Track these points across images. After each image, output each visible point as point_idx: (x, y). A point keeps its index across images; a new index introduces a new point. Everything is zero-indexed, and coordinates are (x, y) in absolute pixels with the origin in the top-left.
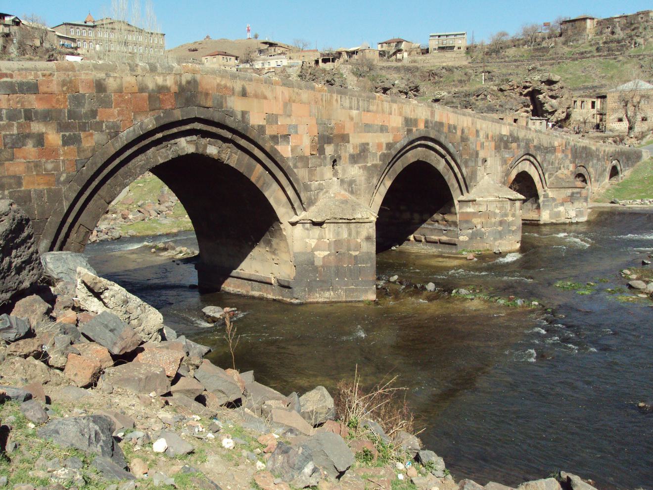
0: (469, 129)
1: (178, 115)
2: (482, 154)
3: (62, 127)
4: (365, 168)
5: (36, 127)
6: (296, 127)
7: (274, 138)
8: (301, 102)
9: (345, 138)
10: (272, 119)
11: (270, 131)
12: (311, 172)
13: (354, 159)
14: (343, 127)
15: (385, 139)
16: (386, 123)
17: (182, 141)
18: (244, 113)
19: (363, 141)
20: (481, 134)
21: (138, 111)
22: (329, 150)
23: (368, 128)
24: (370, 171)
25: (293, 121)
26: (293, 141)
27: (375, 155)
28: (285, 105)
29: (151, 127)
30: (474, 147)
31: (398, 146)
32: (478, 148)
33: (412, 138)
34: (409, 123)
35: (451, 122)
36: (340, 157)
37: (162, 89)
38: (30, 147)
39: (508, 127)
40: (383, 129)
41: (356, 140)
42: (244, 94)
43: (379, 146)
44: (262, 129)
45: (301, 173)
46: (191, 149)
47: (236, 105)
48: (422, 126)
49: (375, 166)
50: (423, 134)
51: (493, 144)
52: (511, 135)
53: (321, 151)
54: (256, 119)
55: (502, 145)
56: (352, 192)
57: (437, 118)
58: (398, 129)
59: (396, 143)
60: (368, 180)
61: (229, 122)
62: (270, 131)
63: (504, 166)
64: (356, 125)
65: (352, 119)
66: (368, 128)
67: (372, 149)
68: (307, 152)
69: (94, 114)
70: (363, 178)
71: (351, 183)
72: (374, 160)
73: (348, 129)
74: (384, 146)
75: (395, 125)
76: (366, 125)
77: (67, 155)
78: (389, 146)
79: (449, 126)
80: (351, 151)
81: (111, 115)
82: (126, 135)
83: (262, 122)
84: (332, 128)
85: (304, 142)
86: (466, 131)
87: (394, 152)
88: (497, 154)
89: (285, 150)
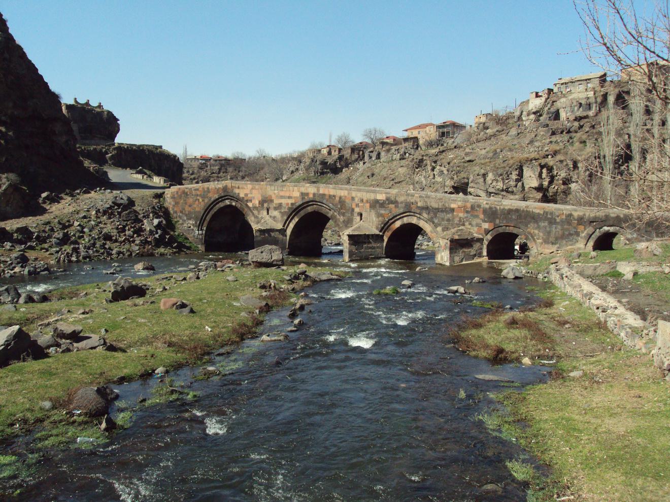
0: (346, 197)
1: (223, 195)
2: (357, 210)
3: (202, 198)
4: (281, 212)
5: (198, 198)
6: (254, 197)
7: (247, 201)
11: (245, 199)
13: (276, 209)
15: (290, 201)
17: (227, 201)
18: (239, 193)
19: (280, 202)
20: (356, 200)
21: (215, 194)
22: (266, 205)
23: (282, 197)
24: (283, 214)
27: (285, 208)
29: (217, 197)
31: (297, 204)
33: (304, 201)
34: (303, 195)
35: (332, 193)
37: (219, 188)
38: (197, 202)
39: (384, 195)
40: (289, 197)
41: (276, 201)
42: (239, 188)
43: (287, 204)
44: (243, 198)
45: (255, 212)
46: (229, 203)
47: (237, 191)
48: (311, 196)
49: (285, 212)
50: (312, 199)
51: (368, 205)
52: (388, 199)
53: (263, 205)
54: (242, 195)
55: (378, 205)
56: (275, 221)
57: (321, 192)
58: (297, 197)
59: (295, 203)
60: (282, 217)
61: (235, 196)
62: (245, 199)
63: (380, 218)
64: (277, 196)
66: (282, 197)
67: (284, 205)
68: (257, 206)
71: (274, 217)
72: (285, 209)
73: (273, 197)
75: (296, 196)
76: (281, 196)
77: (202, 203)
78: (292, 204)
79: (330, 196)
82: (212, 199)
85: (256, 202)
86: (343, 198)
87: (295, 207)
89: (250, 205)
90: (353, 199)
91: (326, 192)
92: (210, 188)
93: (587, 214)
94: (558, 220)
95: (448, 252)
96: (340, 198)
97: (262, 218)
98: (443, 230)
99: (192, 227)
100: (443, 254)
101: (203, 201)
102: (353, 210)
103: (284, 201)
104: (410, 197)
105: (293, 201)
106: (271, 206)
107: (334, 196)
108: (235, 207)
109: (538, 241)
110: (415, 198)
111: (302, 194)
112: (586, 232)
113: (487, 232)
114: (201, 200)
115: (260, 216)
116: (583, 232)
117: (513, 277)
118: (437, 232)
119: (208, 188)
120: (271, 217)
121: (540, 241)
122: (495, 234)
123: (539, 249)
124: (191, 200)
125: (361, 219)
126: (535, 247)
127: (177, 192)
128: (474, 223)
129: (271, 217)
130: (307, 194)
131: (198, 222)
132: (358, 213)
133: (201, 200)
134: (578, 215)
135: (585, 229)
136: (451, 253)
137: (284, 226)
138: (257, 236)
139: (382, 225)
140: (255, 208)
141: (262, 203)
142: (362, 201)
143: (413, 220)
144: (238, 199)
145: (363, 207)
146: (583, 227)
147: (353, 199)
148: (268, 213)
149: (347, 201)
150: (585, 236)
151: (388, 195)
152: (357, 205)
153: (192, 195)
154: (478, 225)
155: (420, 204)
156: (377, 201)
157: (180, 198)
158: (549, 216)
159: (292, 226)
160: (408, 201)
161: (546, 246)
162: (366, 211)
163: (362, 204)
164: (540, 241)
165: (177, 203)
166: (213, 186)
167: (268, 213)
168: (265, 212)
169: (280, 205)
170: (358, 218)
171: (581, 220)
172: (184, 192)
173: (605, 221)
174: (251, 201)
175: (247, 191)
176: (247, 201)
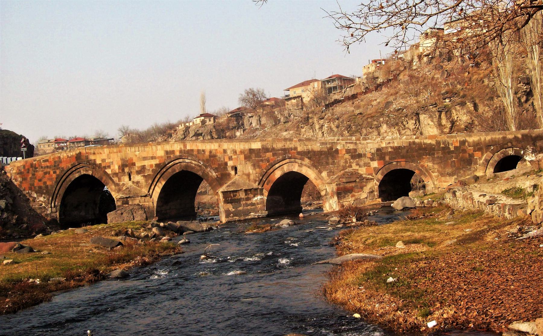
0: (216, 150)
2: (230, 163)
4: (144, 176)
7: (105, 167)
8: (114, 153)
9: (134, 164)
10: (104, 160)
11: (103, 165)
12: (120, 180)
13: (138, 173)
14: (132, 160)
15: (154, 162)
16: (155, 155)
20: (229, 152)
22: (126, 170)
23: (145, 159)
25: (111, 160)
26: (112, 168)
27: (149, 170)
28: (108, 155)
30: (222, 160)
32: (226, 160)
36: (131, 172)
40: (153, 158)
41: (138, 164)
42: (94, 154)
44: (100, 164)
45: (116, 179)
47: (92, 157)
51: (242, 157)
53: (123, 170)
54: (98, 162)
56: (138, 186)
57: (188, 147)
58: (162, 157)
60: (146, 181)
65: (136, 156)
66: (145, 159)
67: (147, 168)
69: (59, 165)
70: (143, 181)
71: (138, 183)
74: (154, 166)
75: (159, 155)
77: (54, 176)
78: (157, 165)
79: (198, 151)
80: (137, 169)
81: (63, 165)
83: (100, 162)
84: (127, 161)
85: (116, 168)
88: (247, 162)
89: (109, 171)
90: (225, 151)
91: (194, 148)
92: (62, 157)
93: (483, 139)
94: (452, 148)
95: (336, 198)
96: (211, 152)
97: (124, 185)
98: (329, 175)
99: (44, 205)
100: (331, 201)
101: (55, 172)
102: (226, 164)
103: (147, 163)
104: (288, 143)
105: (157, 161)
106: (132, 170)
107: (204, 151)
108: (91, 177)
109: (433, 174)
110: (293, 143)
111: (167, 152)
112: (484, 158)
113: (377, 171)
114: (52, 172)
115: (121, 183)
116: (480, 159)
117: (402, 208)
118: (322, 179)
119: (59, 157)
120: (133, 182)
121: (436, 174)
122: (386, 173)
123: (436, 183)
124: (40, 174)
125: (236, 173)
126: (431, 182)
127: (24, 166)
128: (362, 163)
129: (133, 182)
130: (173, 152)
131: (50, 199)
132: (232, 167)
133: (52, 172)
134: (474, 141)
135: (482, 155)
136: (339, 198)
137: (149, 192)
138: (119, 206)
139: (261, 178)
140: (116, 174)
141: (122, 167)
142: (235, 152)
143: (294, 167)
144: (93, 165)
145: (237, 159)
146: (480, 153)
147: (225, 151)
148: (130, 179)
149: (218, 154)
150: (483, 163)
151: (264, 143)
152: (230, 158)
153: (42, 167)
154: (367, 165)
155: (299, 149)
156: (251, 151)
157: (28, 172)
158: (442, 146)
159: (158, 190)
160: (286, 147)
161: (443, 178)
162: (241, 164)
163: (236, 157)
164: (436, 174)
165: (24, 179)
166: (65, 155)
167: (130, 179)
168: (126, 178)
169: (143, 167)
170: (233, 173)
171: (479, 147)
172: (32, 165)
173: (503, 144)
174: (109, 167)
175: (104, 156)
176: (105, 167)
